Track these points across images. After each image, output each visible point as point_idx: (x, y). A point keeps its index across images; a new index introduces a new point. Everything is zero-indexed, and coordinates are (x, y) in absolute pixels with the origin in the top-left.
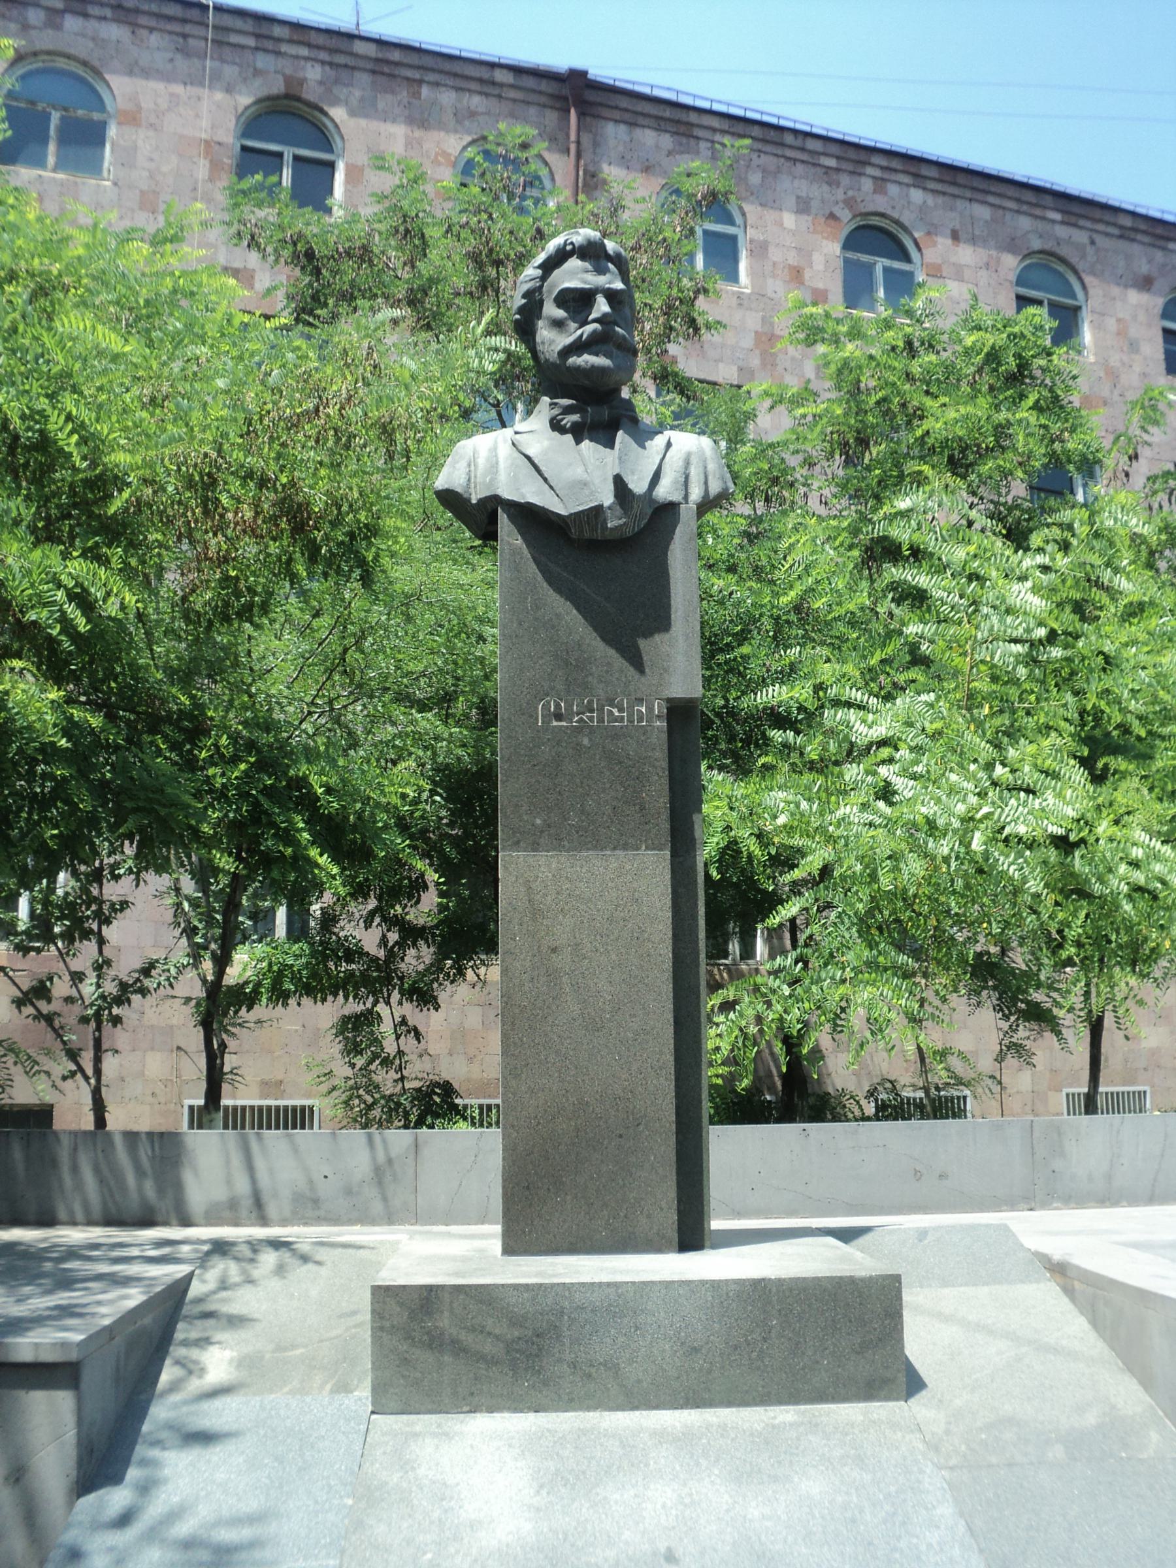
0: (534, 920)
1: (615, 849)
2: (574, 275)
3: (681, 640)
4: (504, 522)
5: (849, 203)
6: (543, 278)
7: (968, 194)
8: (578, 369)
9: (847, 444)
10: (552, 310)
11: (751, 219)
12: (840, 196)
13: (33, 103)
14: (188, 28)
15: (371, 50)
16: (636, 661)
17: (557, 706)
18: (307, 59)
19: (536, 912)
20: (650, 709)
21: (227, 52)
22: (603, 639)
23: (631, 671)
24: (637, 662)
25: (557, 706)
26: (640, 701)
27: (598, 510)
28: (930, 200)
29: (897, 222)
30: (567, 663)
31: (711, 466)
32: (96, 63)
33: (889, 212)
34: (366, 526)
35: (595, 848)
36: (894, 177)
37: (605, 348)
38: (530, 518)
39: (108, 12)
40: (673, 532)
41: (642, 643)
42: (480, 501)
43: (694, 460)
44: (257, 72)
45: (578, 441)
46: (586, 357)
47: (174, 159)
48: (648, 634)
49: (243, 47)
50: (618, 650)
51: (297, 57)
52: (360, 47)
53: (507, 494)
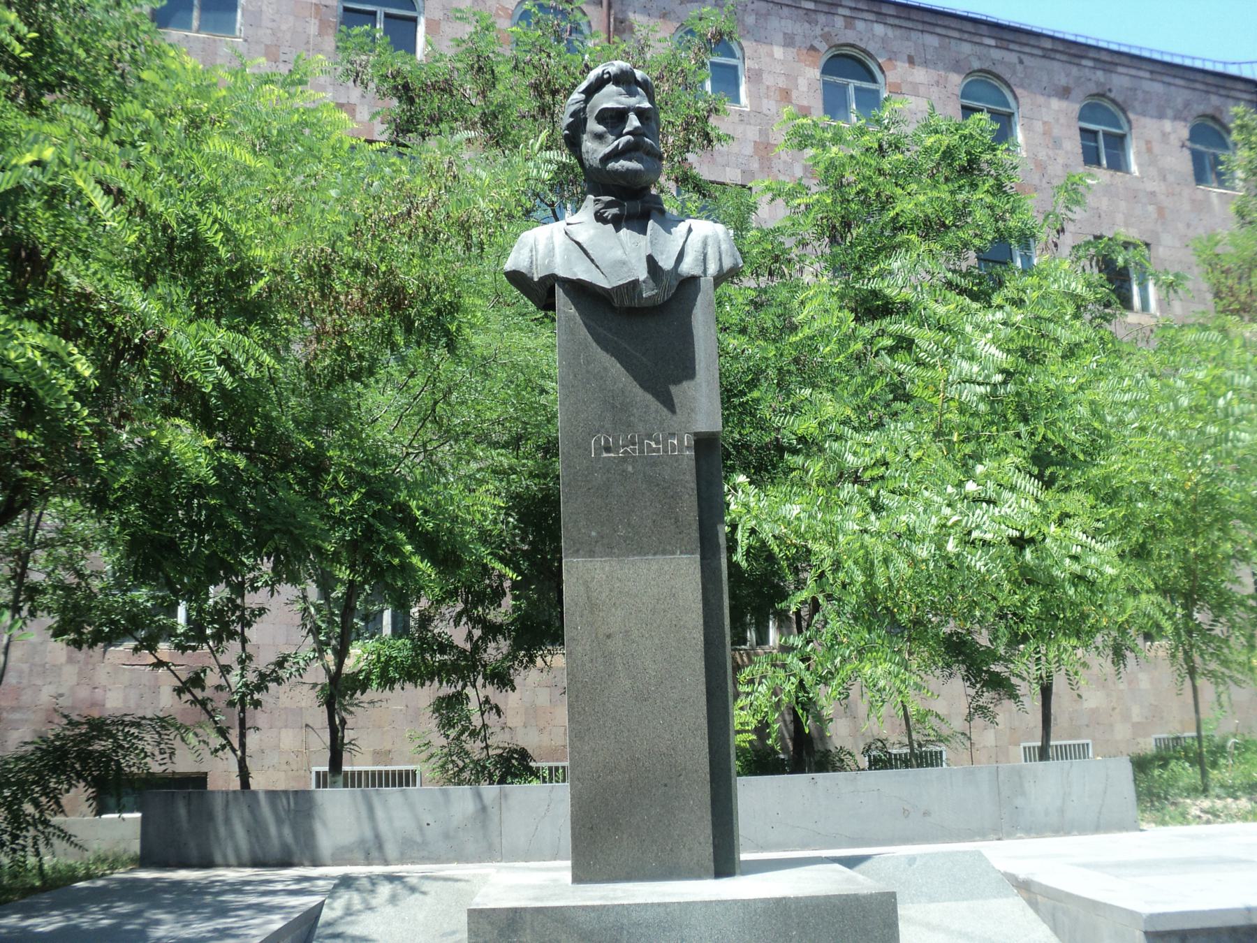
0: (592, 612)
1: (655, 554)
2: (611, 97)
3: (704, 385)
4: (559, 292)
5: (826, 37)
6: (586, 101)
7: (920, 27)
8: (616, 172)
9: (834, 227)
10: (593, 126)
11: (748, 52)
12: (818, 31)
16: (668, 403)
17: (607, 441)
19: (593, 606)
20: (681, 441)
22: (641, 385)
23: (665, 412)
24: (669, 403)
25: (607, 441)
26: (673, 435)
27: (635, 284)
28: (890, 32)
29: (864, 51)
30: (613, 407)
31: (724, 247)
33: (858, 43)
34: (450, 303)
35: (639, 554)
36: (860, 15)
37: (637, 154)
38: (581, 291)
40: (695, 300)
41: (674, 389)
42: (541, 278)
43: (710, 242)
45: (618, 229)
46: (622, 162)
47: (291, 18)
48: (678, 381)
50: (653, 395)
53: (561, 273)
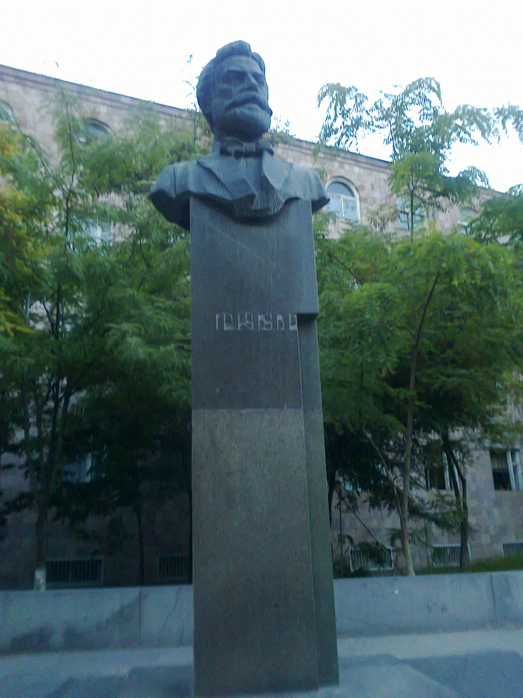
7: (378, 169)
14: (48, 88)
15: (129, 101)
18: (100, 104)
28: (362, 171)
29: (349, 180)
33: (346, 176)
36: (347, 161)
39: (12, 79)
52: (124, 100)
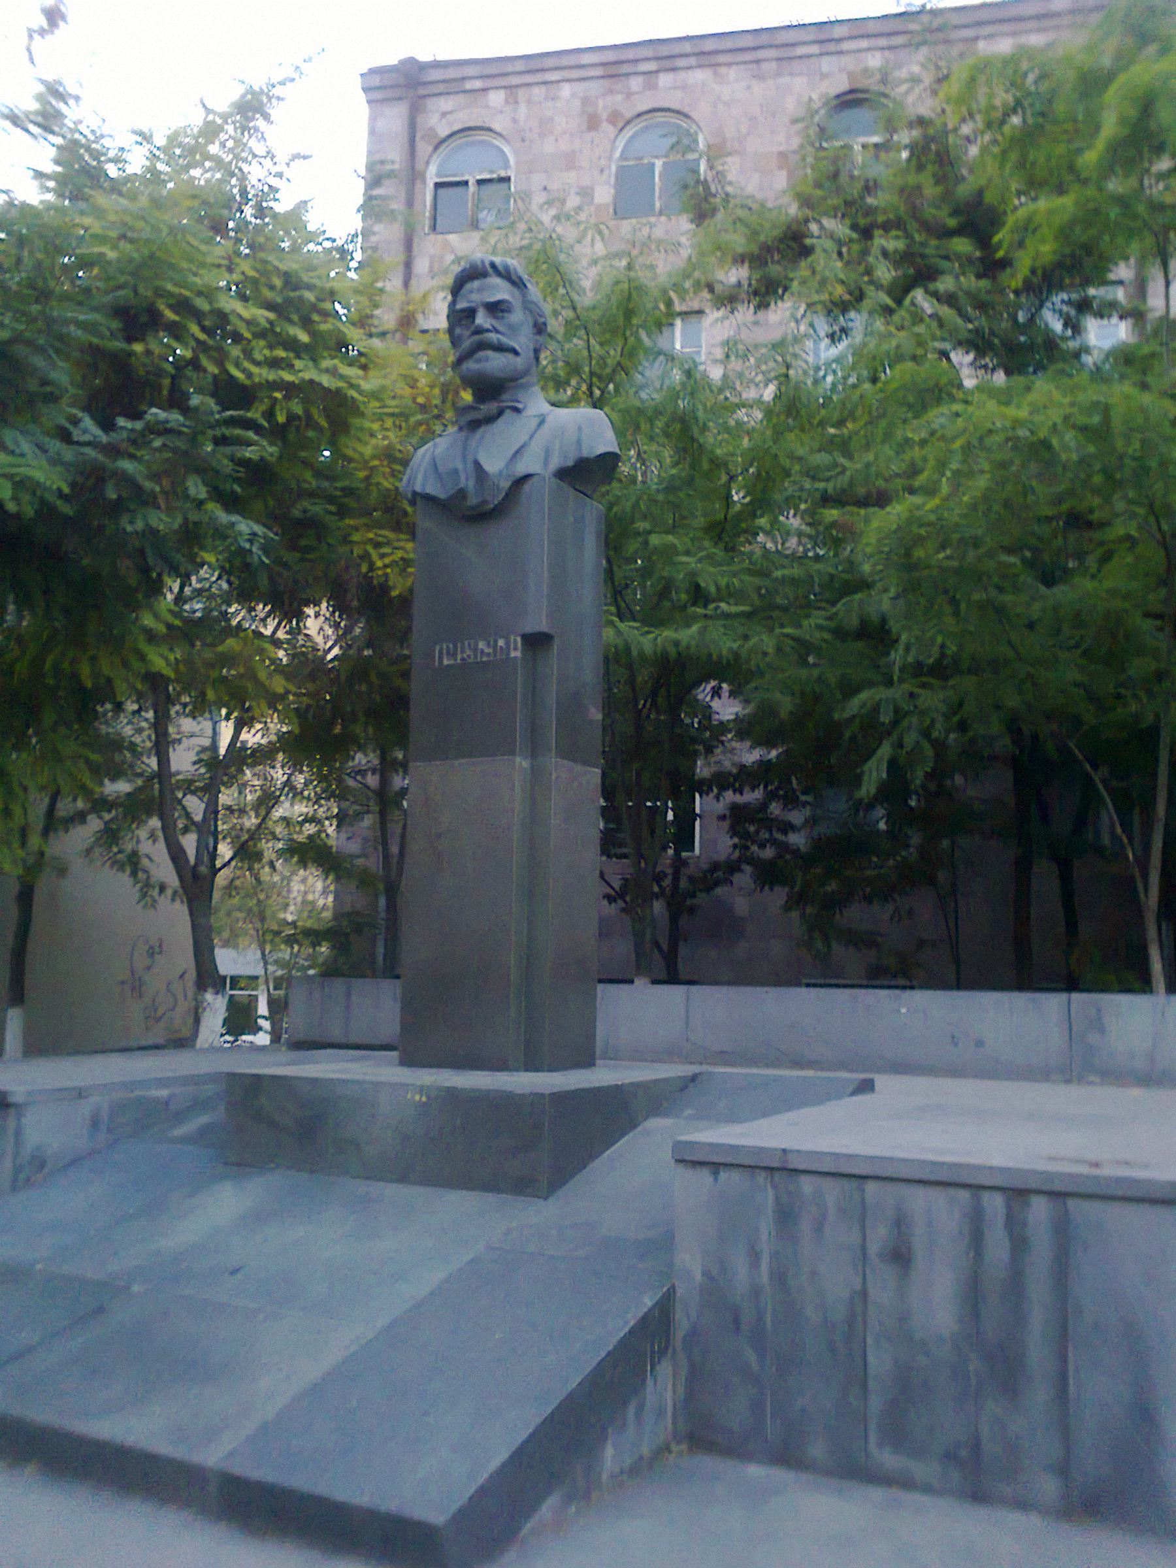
13: (641, 158)
18: (868, 49)
21: (796, 66)
32: (686, 110)
44: (824, 76)
47: (757, 176)
49: (809, 56)
51: (859, 51)
